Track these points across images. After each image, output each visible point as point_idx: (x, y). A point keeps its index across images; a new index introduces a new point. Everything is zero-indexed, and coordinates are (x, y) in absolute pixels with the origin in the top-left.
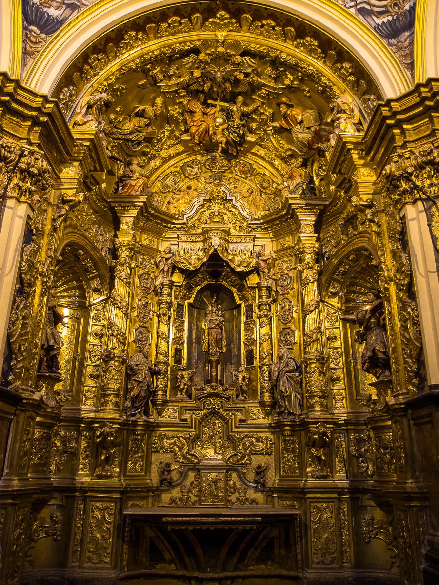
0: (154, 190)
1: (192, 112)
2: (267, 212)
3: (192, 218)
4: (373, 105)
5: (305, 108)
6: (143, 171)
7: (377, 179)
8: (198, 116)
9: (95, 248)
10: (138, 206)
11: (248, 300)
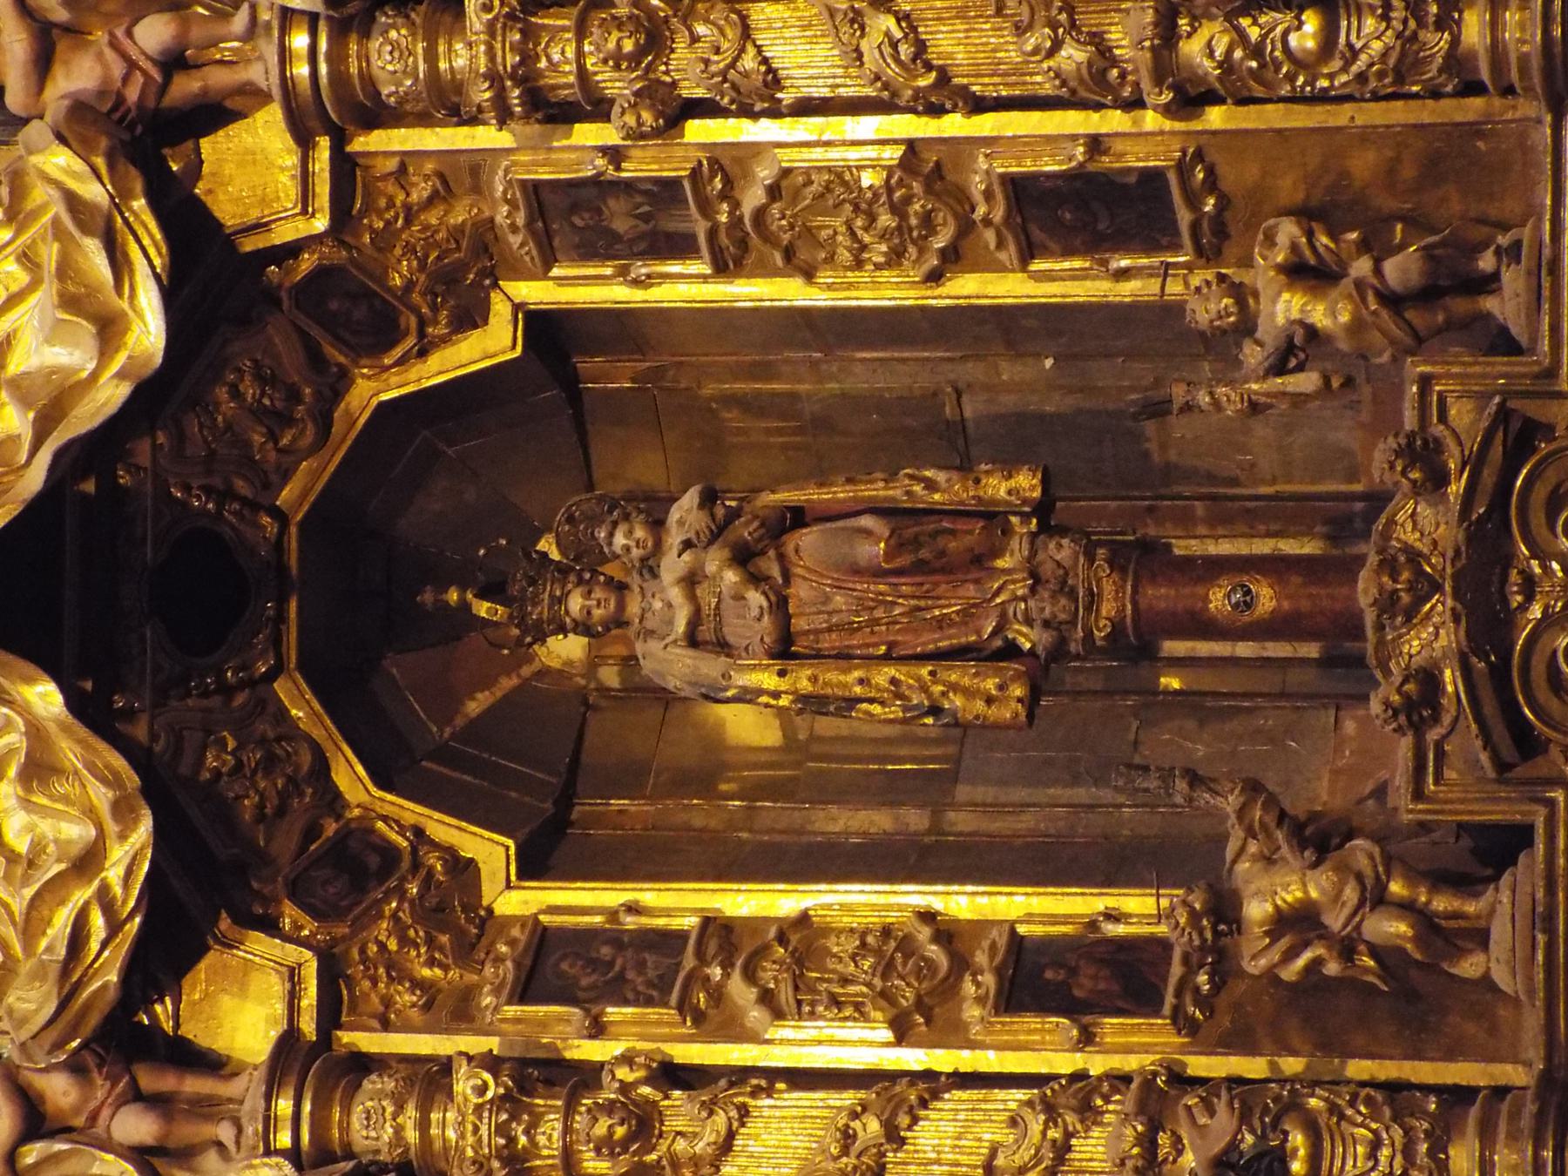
11: (483, 239)
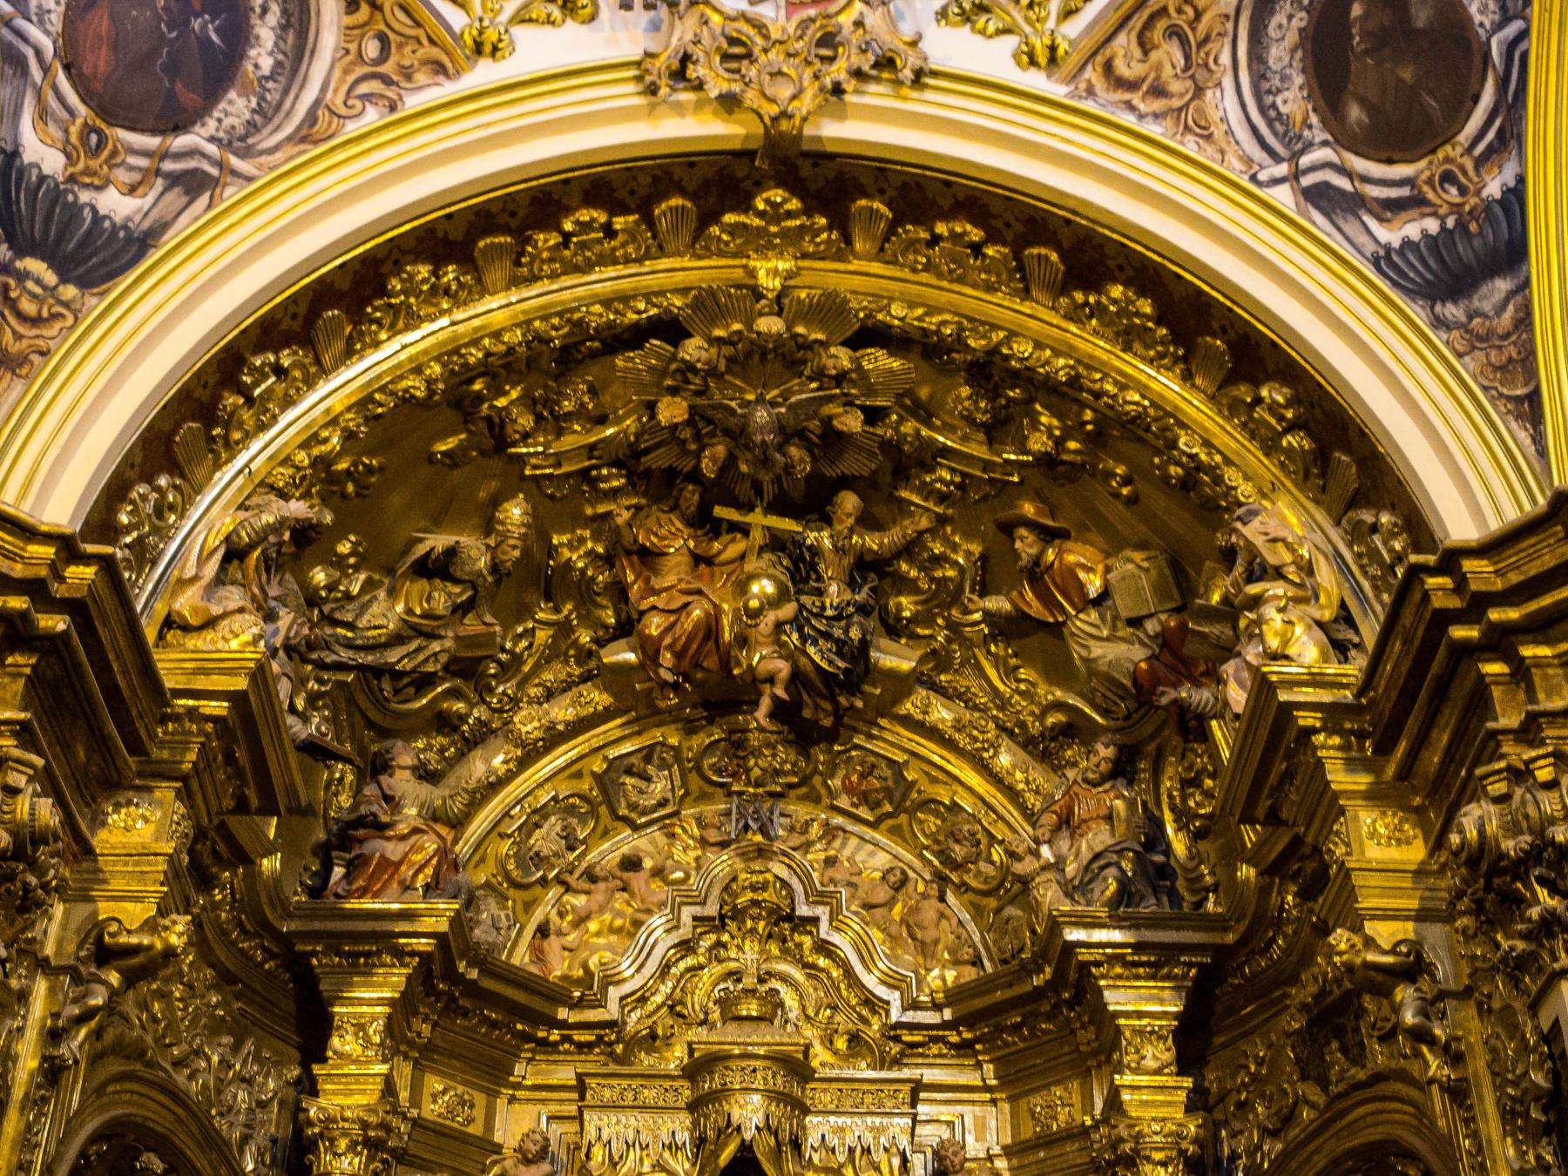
0: (481, 878)
1: (648, 557)
2: (970, 974)
3: (643, 1000)
4: (1391, 550)
5: (1114, 545)
6: (436, 795)
7: (1431, 854)
8: (674, 572)
9: (213, 1142)
10: (413, 954)
